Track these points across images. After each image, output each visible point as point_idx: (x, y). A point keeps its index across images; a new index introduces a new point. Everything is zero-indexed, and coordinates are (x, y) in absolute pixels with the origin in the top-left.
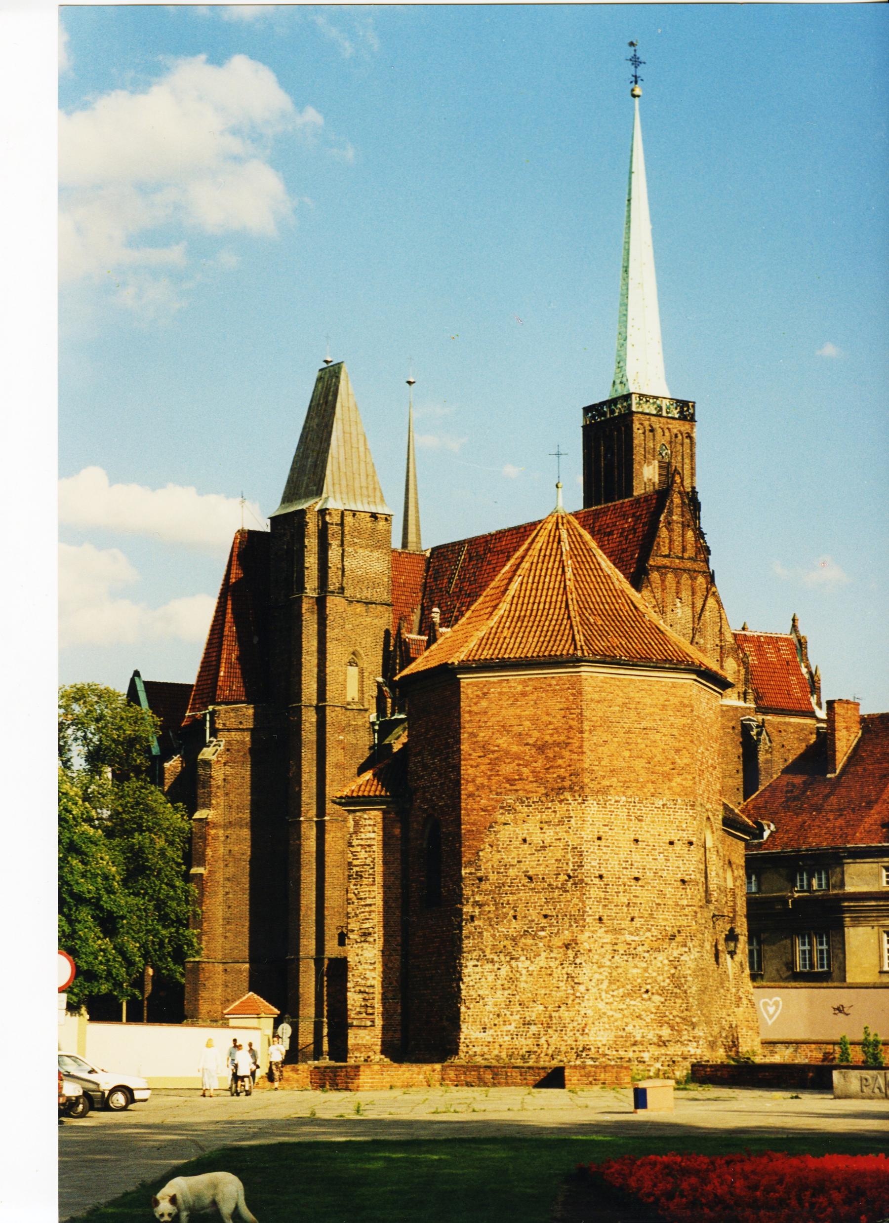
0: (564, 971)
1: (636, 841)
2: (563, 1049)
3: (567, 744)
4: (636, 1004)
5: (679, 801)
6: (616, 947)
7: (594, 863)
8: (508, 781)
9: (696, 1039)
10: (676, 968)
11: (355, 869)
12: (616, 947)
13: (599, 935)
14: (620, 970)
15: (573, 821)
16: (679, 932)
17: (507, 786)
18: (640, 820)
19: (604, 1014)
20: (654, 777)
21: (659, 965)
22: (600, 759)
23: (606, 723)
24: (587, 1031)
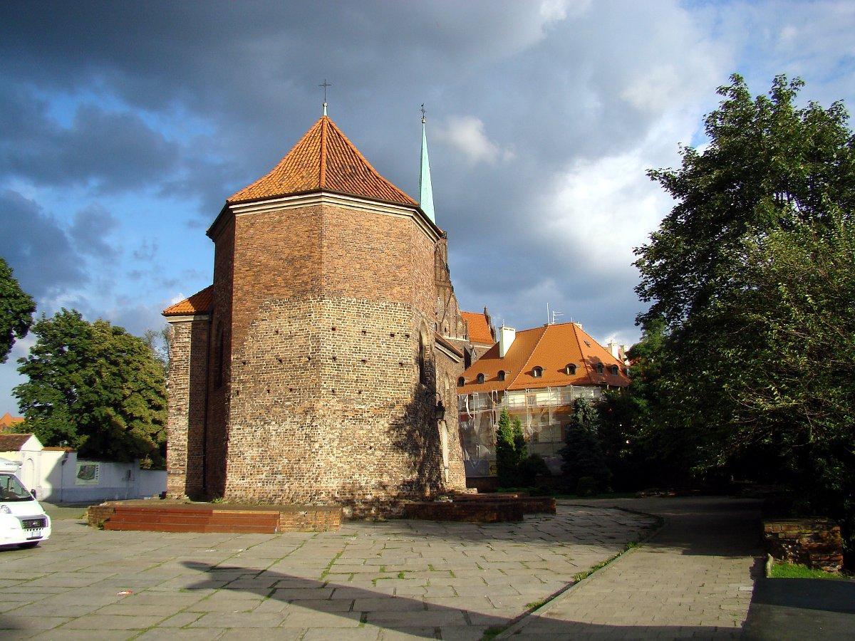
0: (303, 433)
3: (310, 257)
4: (362, 457)
5: (399, 305)
6: (346, 414)
7: (328, 347)
8: (266, 288)
12: (346, 414)
13: (332, 404)
15: (313, 315)
16: (397, 402)
18: (367, 317)
19: (335, 465)
23: (342, 241)
24: (319, 479)
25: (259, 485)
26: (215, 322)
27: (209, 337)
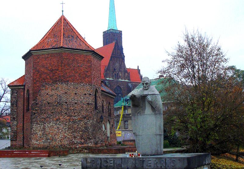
1: (76, 94)
2: (56, 145)
4: (76, 134)
9: (91, 142)
10: (86, 125)
11: (12, 103)
12: (70, 120)
14: (71, 126)
15: (59, 89)
16: (87, 116)
17: (44, 80)
20: (81, 78)
21: (82, 124)
22: (66, 73)
25: (42, 143)
26: (26, 89)
27: (24, 94)
